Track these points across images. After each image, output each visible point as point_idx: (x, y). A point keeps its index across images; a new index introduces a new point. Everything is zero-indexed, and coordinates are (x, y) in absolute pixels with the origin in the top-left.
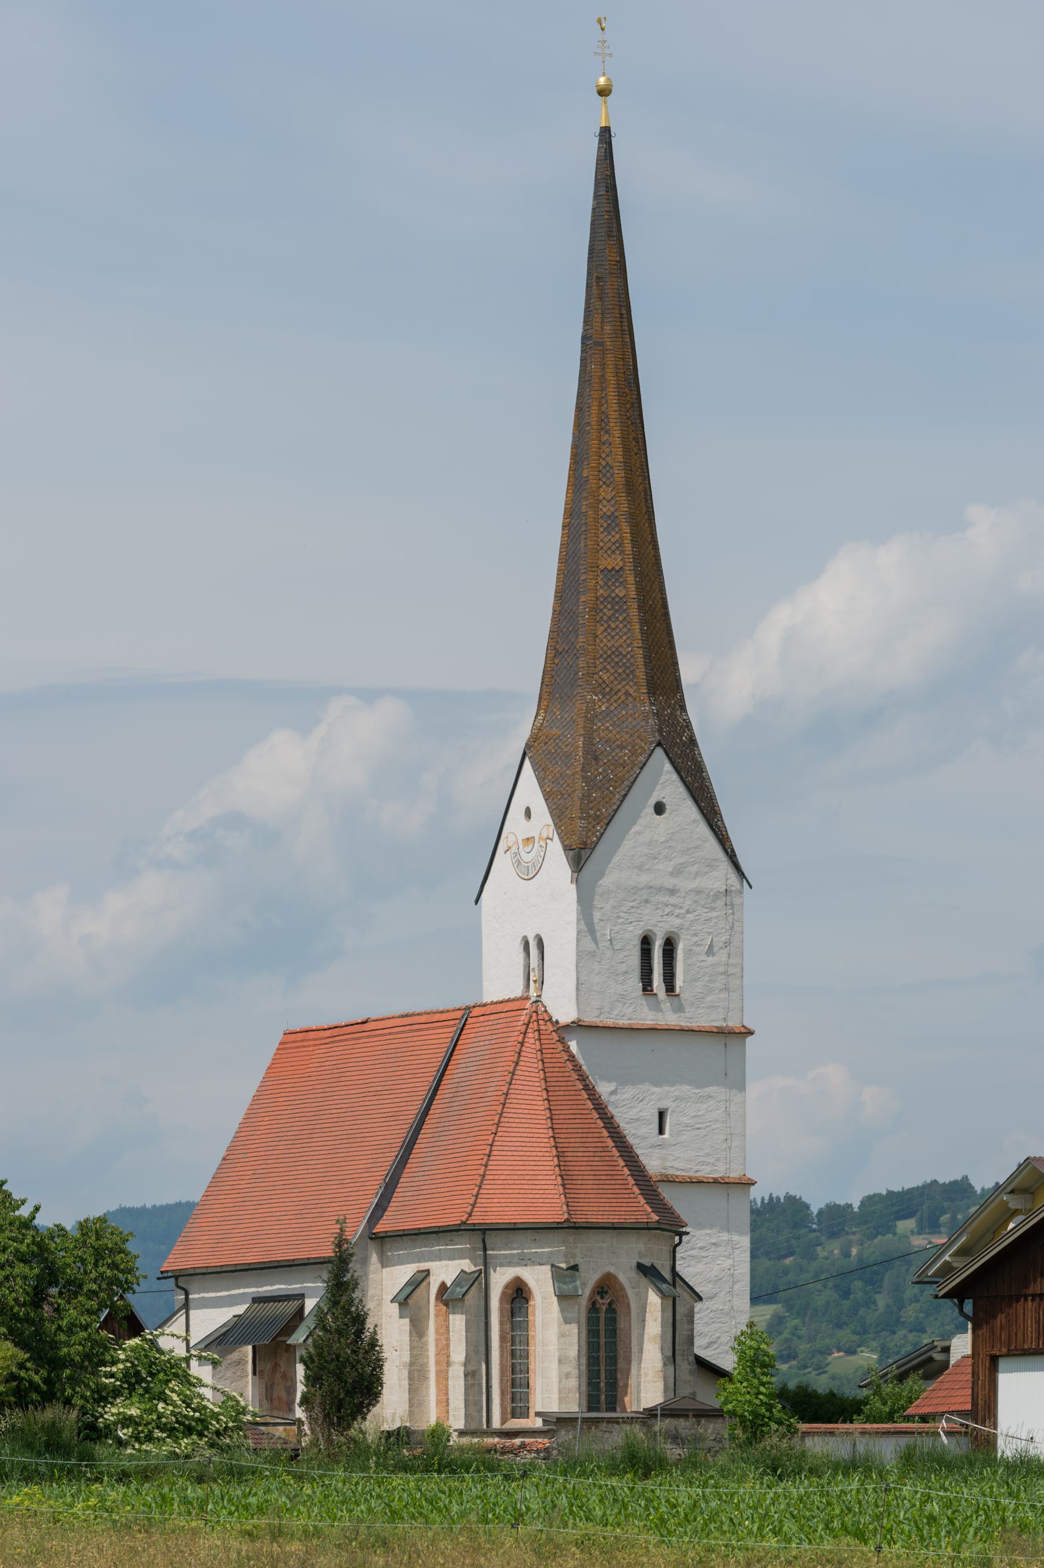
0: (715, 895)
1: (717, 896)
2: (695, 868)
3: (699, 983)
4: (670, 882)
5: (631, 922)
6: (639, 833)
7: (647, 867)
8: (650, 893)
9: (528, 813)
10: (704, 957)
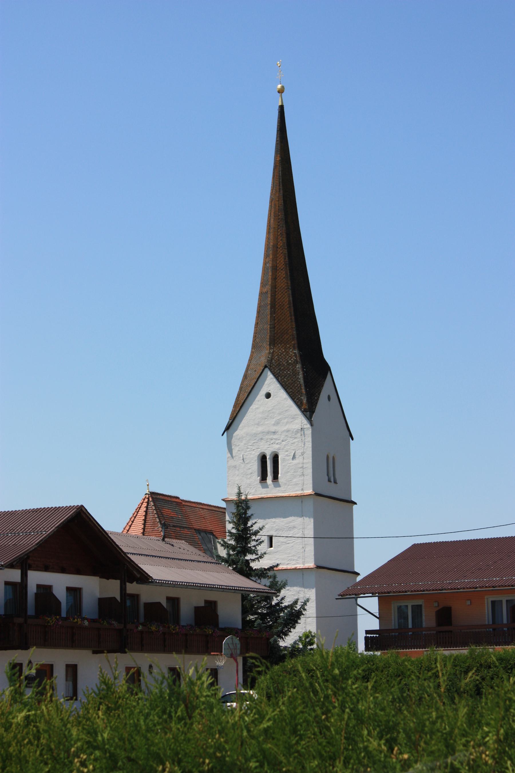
0: (296, 431)
1: (297, 432)
2: (286, 420)
3: (289, 474)
4: (273, 429)
5: (254, 450)
6: (257, 408)
7: (261, 423)
8: (264, 435)
9: (329, 398)
10: (292, 461)
